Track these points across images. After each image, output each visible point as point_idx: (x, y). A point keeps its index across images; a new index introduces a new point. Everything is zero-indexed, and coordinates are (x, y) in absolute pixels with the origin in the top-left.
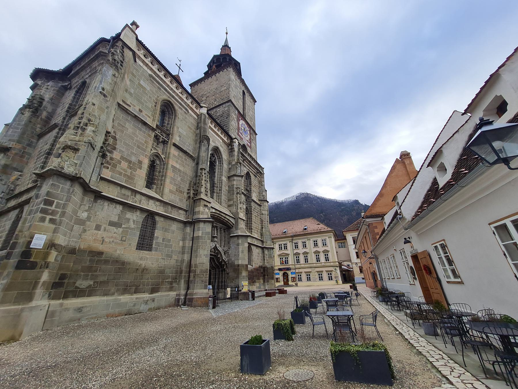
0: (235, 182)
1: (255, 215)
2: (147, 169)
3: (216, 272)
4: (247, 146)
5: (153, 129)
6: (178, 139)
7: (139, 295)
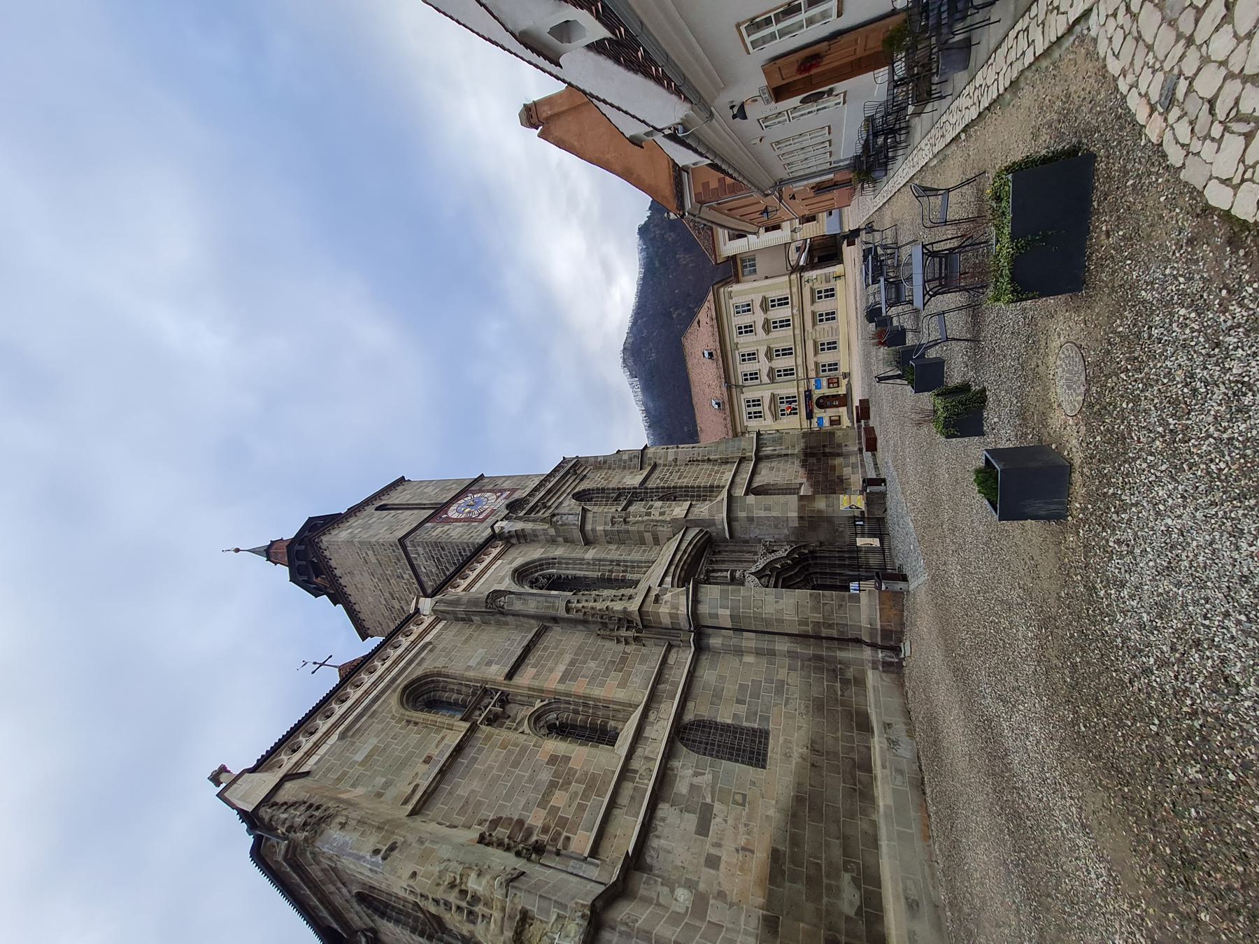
0: (598, 528)
1: (679, 479)
2: (570, 743)
3: (817, 573)
4: (511, 500)
5: (473, 729)
6: (494, 668)
7: (875, 761)
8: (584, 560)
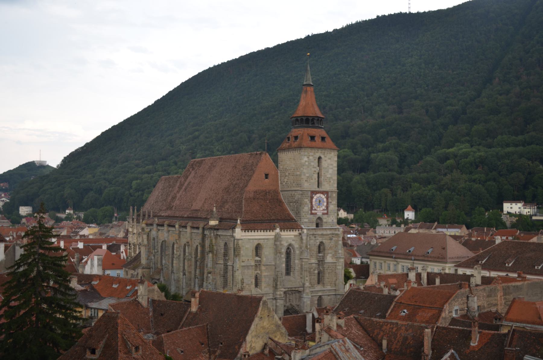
1: (328, 273)
8: (295, 260)
